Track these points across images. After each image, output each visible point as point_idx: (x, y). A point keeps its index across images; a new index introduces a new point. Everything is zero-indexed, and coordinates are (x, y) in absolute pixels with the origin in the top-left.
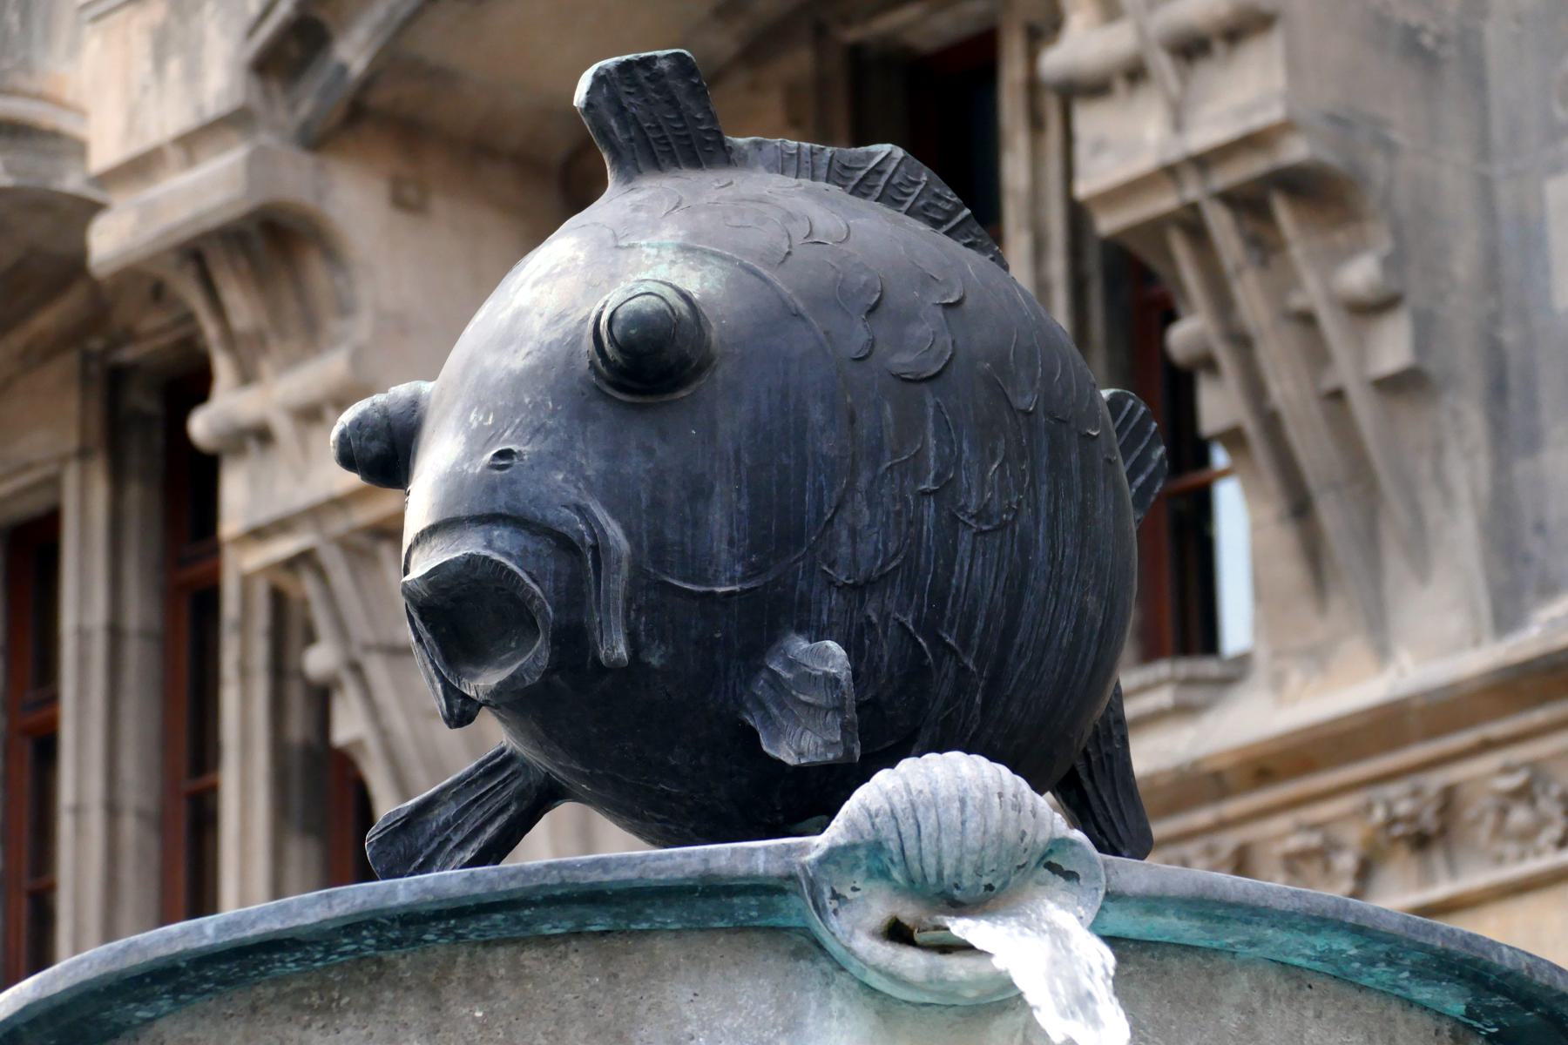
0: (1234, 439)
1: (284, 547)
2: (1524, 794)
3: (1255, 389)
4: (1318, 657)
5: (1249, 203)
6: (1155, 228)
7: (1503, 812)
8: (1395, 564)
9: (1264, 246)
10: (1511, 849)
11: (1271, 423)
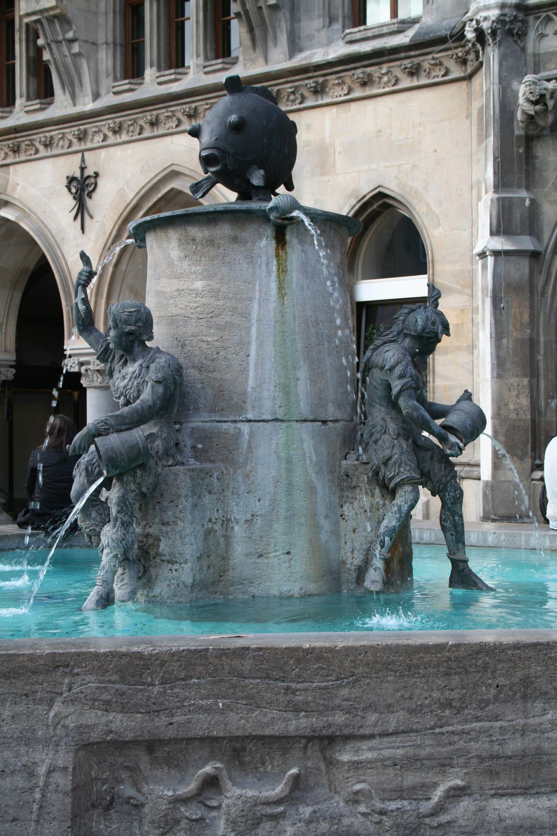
2: (293, 93)
4: (253, 61)
7: (289, 96)
8: (270, 44)
10: (290, 103)
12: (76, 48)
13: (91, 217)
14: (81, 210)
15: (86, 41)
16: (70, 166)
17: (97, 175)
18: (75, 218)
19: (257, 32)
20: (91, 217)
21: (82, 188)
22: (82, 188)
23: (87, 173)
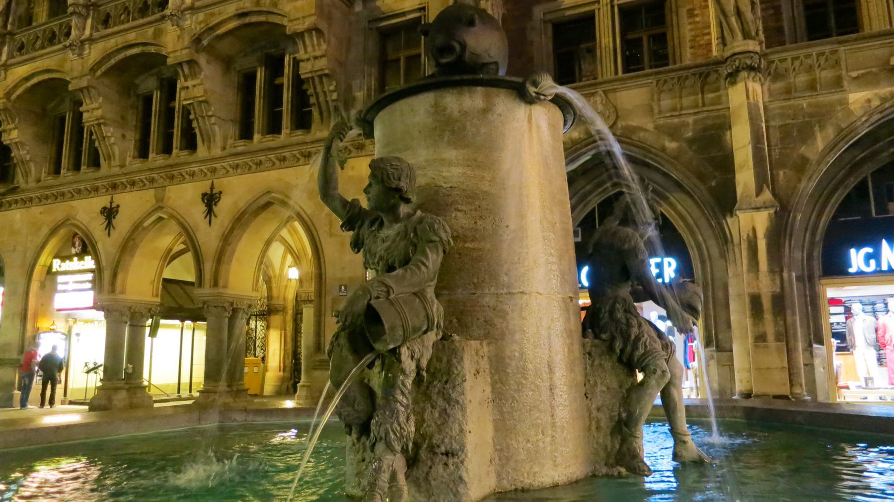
0: (314, 104)
1: (188, 102)
3: (317, 98)
5: (320, 77)
6: (308, 79)
9: (321, 83)
11: (319, 103)
12: (213, 120)
13: (216, 216)
14: (210, 212)
15: (219, 118)
16: (204, 186)
17: (221, 192)
18: (206, 217)
19: (325, 114)
20: (216, 216)
22: (210, 200)
23: (215, 191)
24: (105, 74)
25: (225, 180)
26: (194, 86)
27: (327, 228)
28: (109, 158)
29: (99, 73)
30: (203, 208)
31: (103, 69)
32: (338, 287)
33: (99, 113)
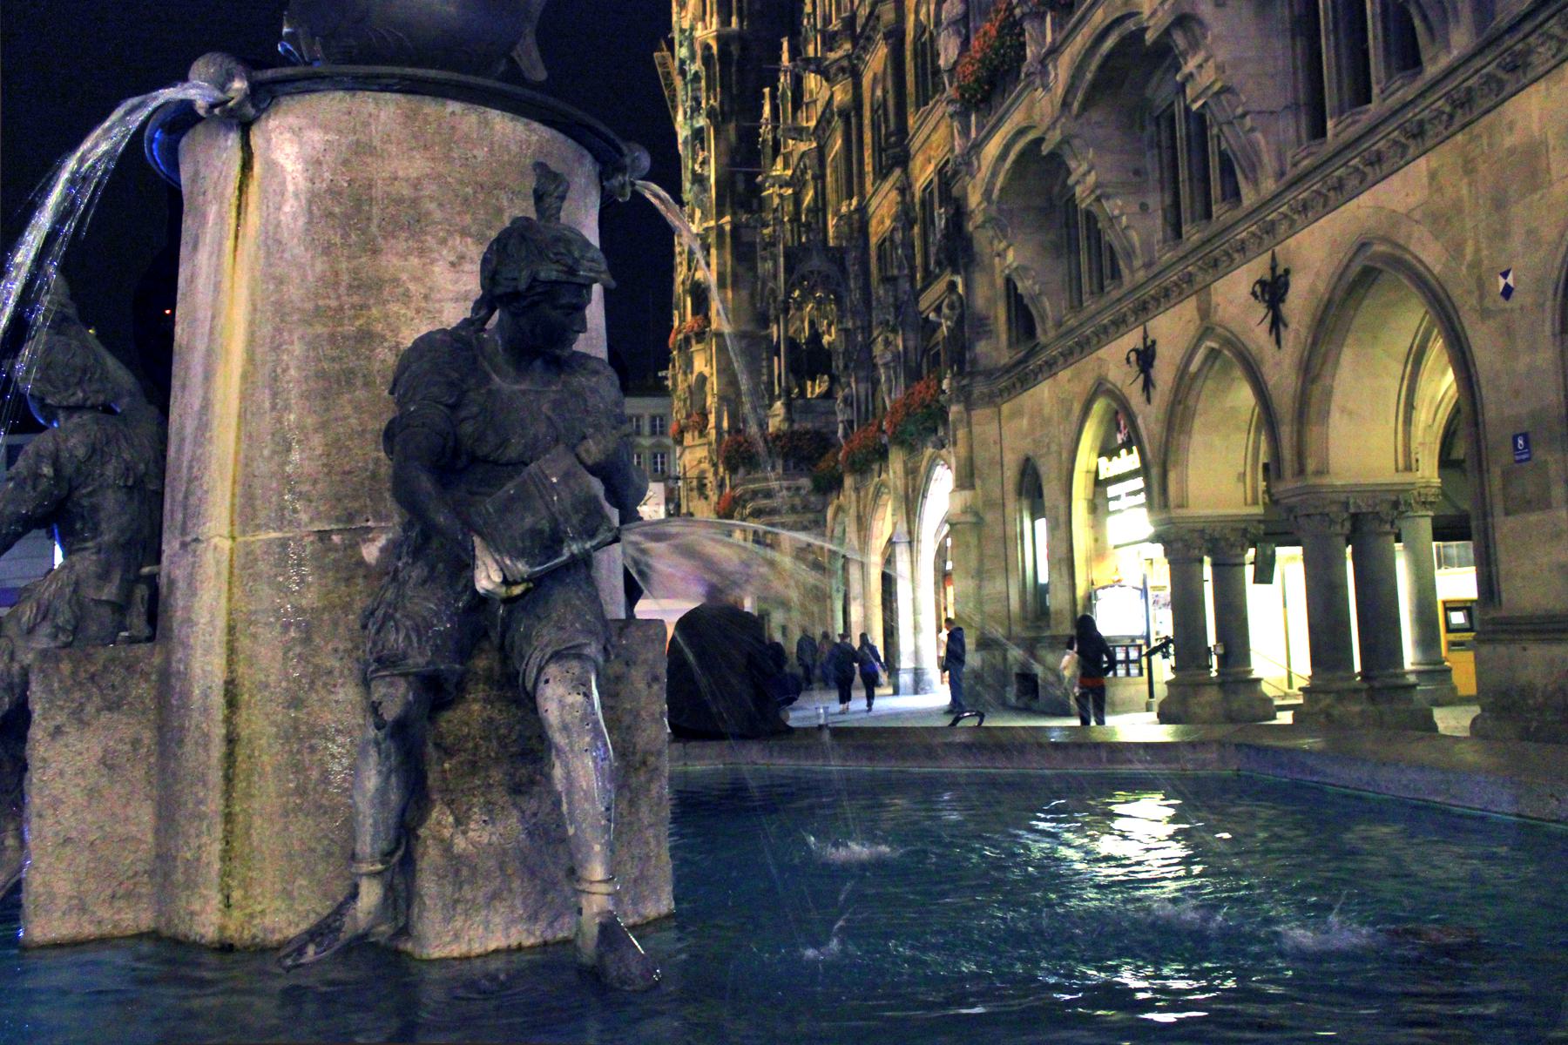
1: (1200, 102)
12: (1248, 121)
17: (1287, 272)
21: (1273, 290)
22: (1273, 290)
24: (1085, 106)
25: (1291, 242)
26: (1200, 66)
27: (1474, 301)
28: (1130, 254)
29: (1076, 105)
30: (1261, 310)
31: (1080, 96)
32: (1509, 443)
33: (1091, 179)
